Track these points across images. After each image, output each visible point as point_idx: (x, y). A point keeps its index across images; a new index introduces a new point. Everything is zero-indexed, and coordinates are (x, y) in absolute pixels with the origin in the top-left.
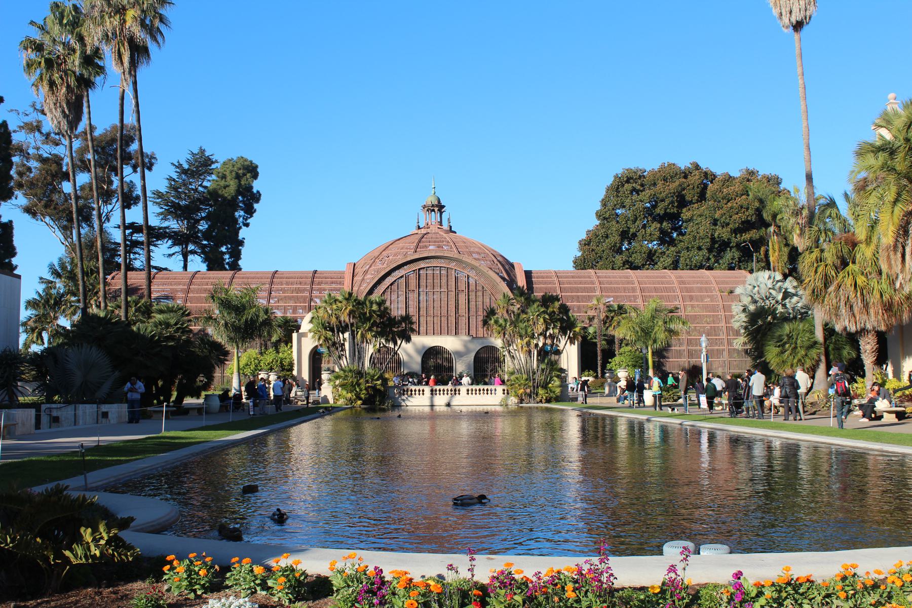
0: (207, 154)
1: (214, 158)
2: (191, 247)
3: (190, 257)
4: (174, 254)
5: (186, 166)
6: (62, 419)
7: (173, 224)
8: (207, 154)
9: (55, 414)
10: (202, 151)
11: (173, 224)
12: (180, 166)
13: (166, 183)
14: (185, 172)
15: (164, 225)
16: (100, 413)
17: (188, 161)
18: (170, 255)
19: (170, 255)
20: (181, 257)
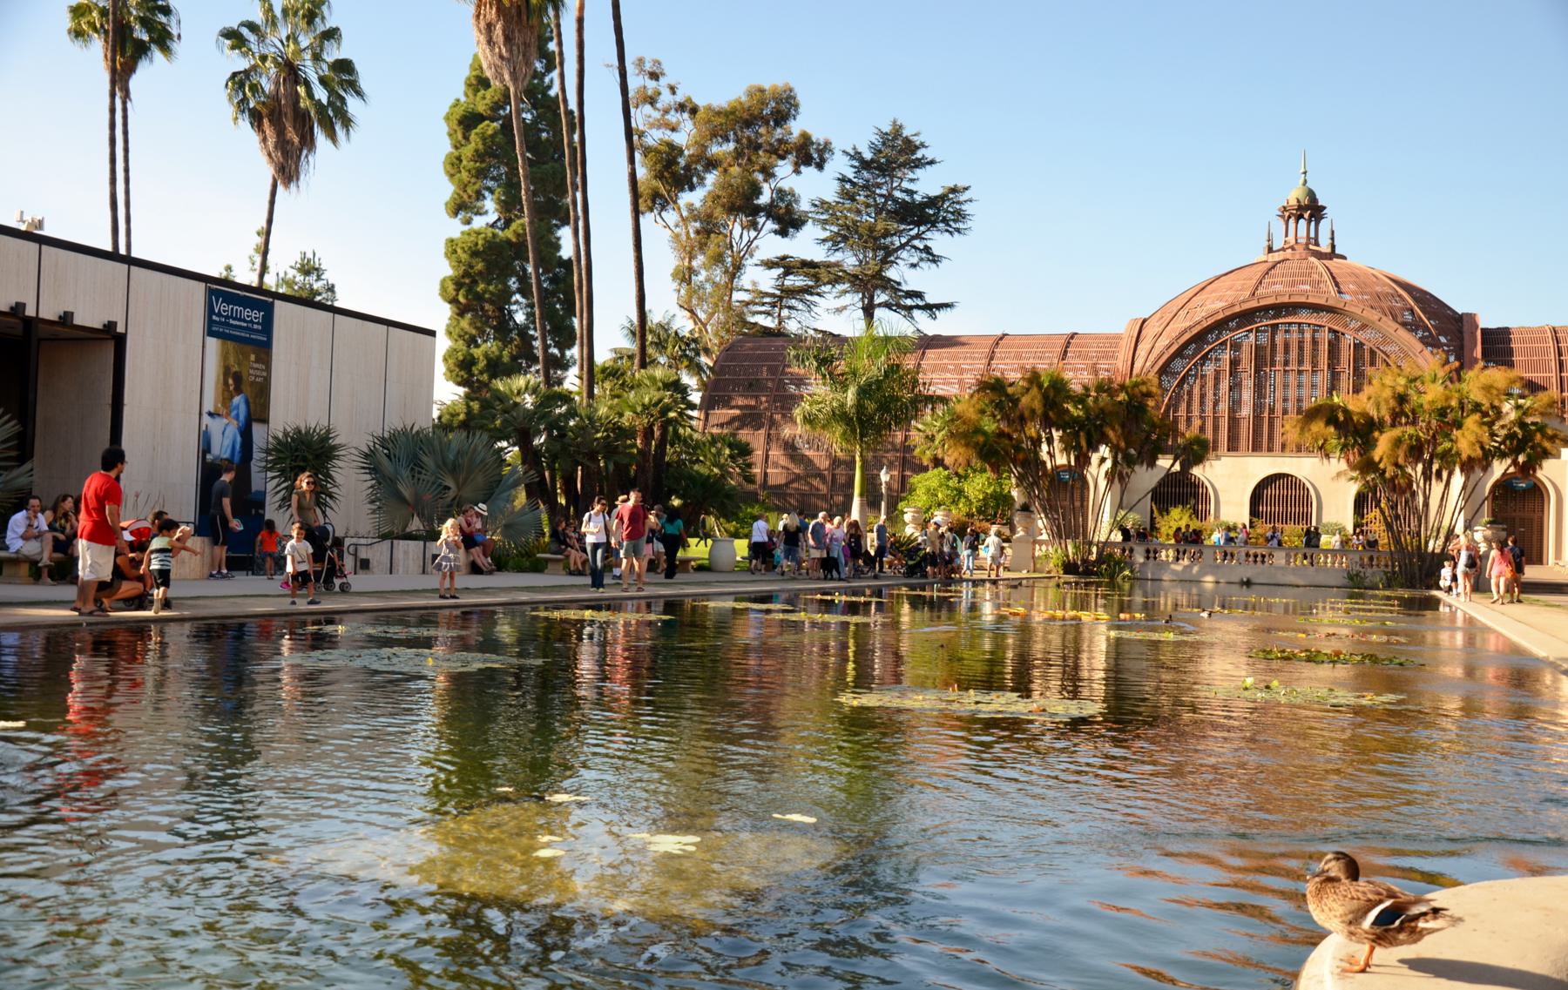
0: (906, 133)
1: (917, 140)
2: (881, 297)
3: (878, 313)
4: (845, 308)
5: (868, 156)
6: (373, 563)
7: (848, 259)
8: (906, 133)
9: (363, 554)
10: (897, 130)
11: (848, 259)
12: (857, 156)
13: (836, 186)
14: (865, 165)
15: (837, 257)
16: (429, 556)
17: (872, 146)
18: (839, 310)
19: (839, 310)
20: (861, 313)
